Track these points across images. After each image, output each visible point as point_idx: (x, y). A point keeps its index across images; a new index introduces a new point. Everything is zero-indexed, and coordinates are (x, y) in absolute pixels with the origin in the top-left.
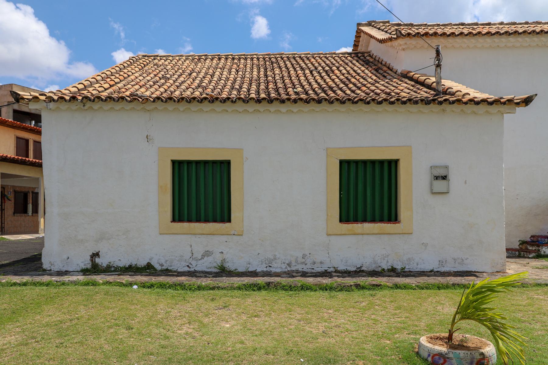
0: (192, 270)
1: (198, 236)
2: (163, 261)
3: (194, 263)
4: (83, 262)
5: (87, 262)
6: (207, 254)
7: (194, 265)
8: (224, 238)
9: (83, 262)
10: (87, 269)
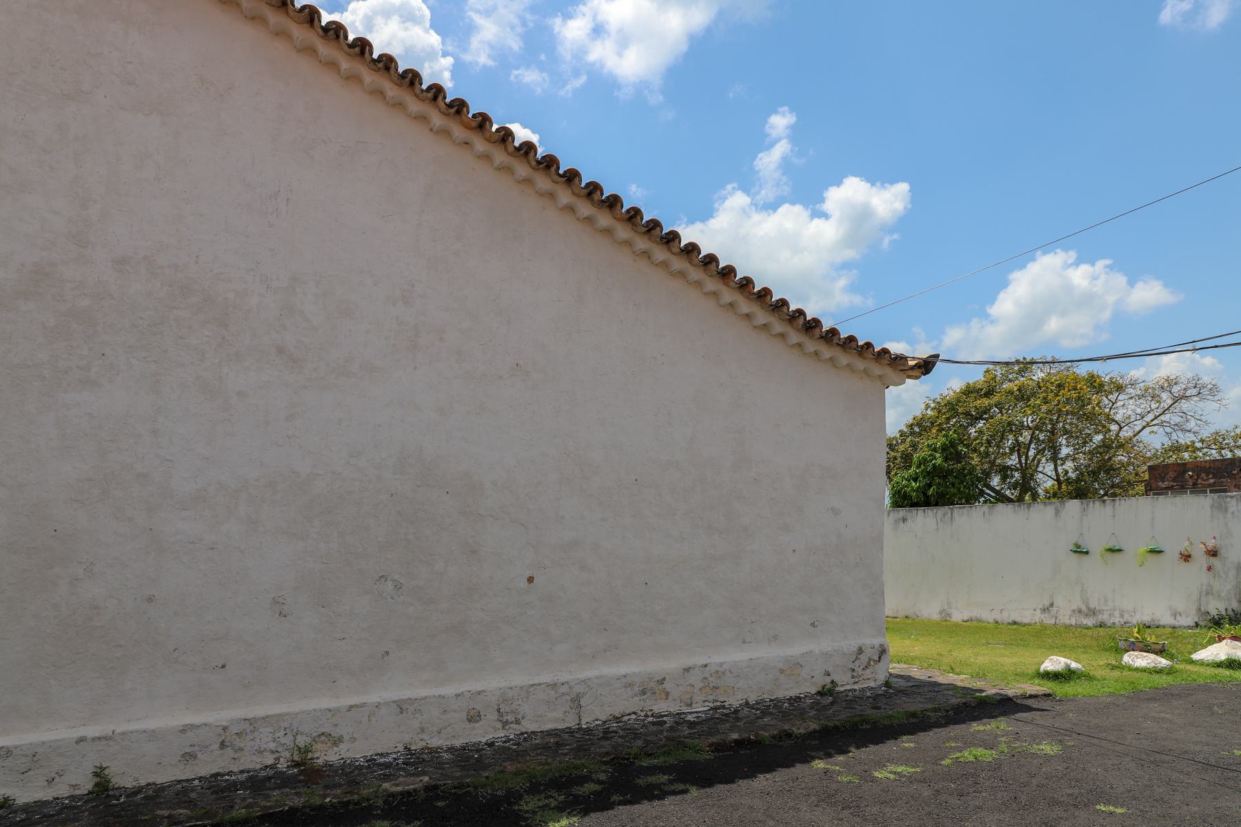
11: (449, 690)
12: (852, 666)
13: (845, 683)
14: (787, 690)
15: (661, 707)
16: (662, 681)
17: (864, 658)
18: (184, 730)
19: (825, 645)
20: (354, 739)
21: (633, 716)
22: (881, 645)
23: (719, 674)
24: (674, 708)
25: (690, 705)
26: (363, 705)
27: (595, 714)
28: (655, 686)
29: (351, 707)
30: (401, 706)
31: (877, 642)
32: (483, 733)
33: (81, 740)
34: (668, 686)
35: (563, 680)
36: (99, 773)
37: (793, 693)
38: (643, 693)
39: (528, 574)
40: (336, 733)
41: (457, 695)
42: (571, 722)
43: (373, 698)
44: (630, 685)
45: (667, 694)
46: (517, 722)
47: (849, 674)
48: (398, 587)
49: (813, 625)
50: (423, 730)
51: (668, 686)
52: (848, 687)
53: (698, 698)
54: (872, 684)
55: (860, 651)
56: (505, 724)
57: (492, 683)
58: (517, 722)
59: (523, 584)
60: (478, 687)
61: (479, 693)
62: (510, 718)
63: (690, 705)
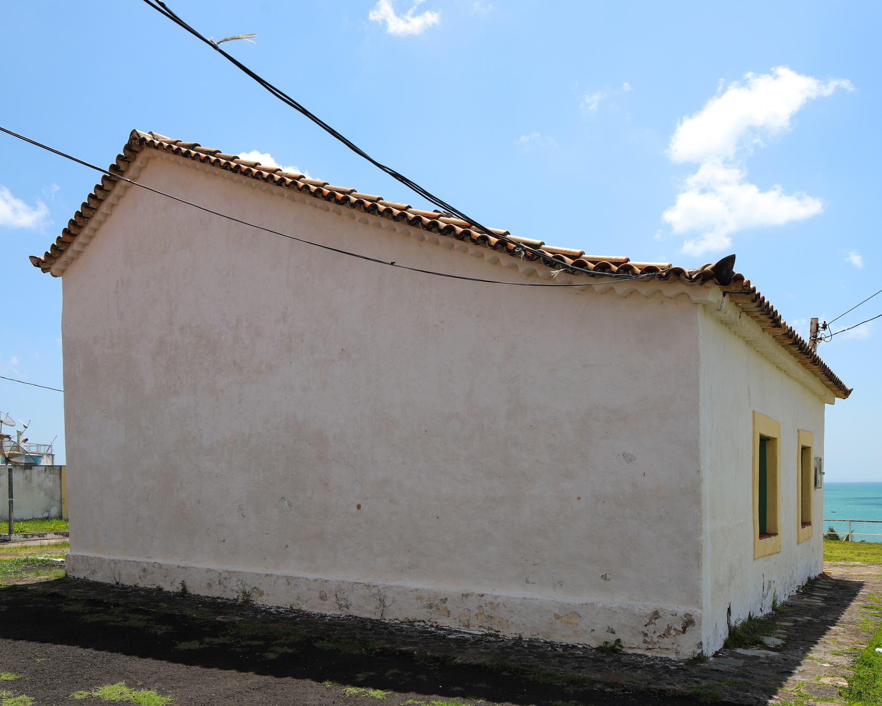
11: (312, 576)
12: (645, 629)
13: (633, 644)
14: (563, 636)
15: (445, 622)
16: (445, 600)
17: (661, 625)
19: (617, 601)
20: (268, 595)
21: (422, 624)
22: (687, 615)
23: (493, 605)
24: (454, 626)
25: (468, 626)
26: (271, 575)
27: (395, 614)
28: (438, 603)
29: (267, 575)
30: (289, 580)
31: (682, 610)
32: (329, 609)
33: (179, 567)
34: (448, 605)
35: (375, 583)
36: (183, 584)
37: (570, 641)
38: (430, 606)
39: (358, 502)
40: (261, 588)
41: (315, 580)
42: (377, 617)
43: (278, 573)
44: (420, 598)
45: (449, 612)
46: (347, 607)
47: (641, 638)
48: (290, 505)
49: (604, 577)
50: (298, 598)
51: (448, 605)
52: (639, 652)
53: (475, 622)
54: (673, 656)
55: (656, 615)
56: (341, 606)
57: (335, 576)
58: (347, 607)
59: (355, 510)
60: (324, 577)
61: (326, 581)
62: (343, 603)
63: (468, 626)
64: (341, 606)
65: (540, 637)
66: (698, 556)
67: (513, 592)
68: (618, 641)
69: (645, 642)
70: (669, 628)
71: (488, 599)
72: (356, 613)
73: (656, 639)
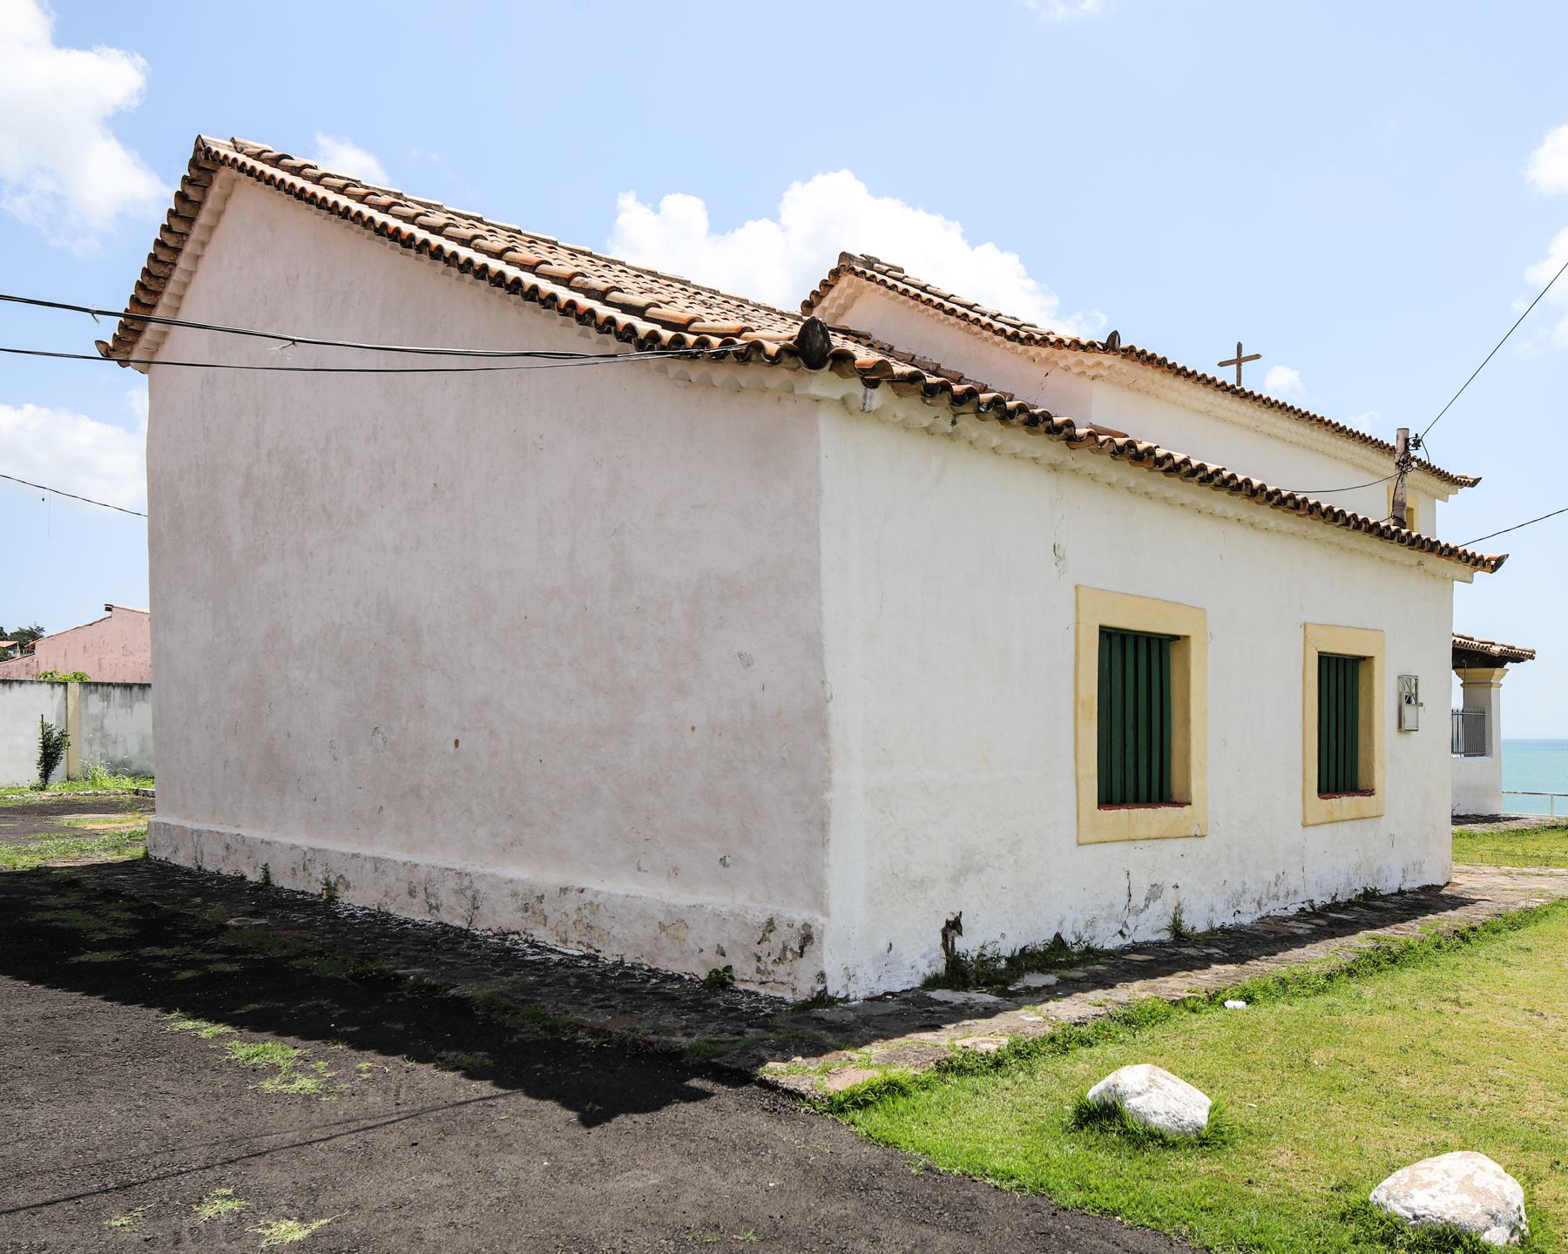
0: (1129, 941)
1: (1139, 844)
2: (1080, 927)
3: (1131, 922)
4: (924, 956)
5: (934, 955)
6: (1155, 892)
7: (1132, 927)
8: (1176, 846)
9: (924, 956)
10: (936, 976)
11: (402, 857)
12: (756, 949)
16: (541, 898)
18: (293, 847)
23: (594, 908)
25: (565, 942)
28: (532, 904)
35: (469, 869)
37: (675, 968)
44: (514, 895)
52: (752, 987)
53: (574, 936)
54: (789, 997)
55: (770, 925)
57: (430, 859)
63: (565, 942)
64: (431, 907)
65: (644, 961)
66: (824, 826)
67: (615, 886)
68: (728, 969)
69: (759, 971)
70: (785, 949)
71: (587, 896)
72: (446, 918)
73: (770, 967)
